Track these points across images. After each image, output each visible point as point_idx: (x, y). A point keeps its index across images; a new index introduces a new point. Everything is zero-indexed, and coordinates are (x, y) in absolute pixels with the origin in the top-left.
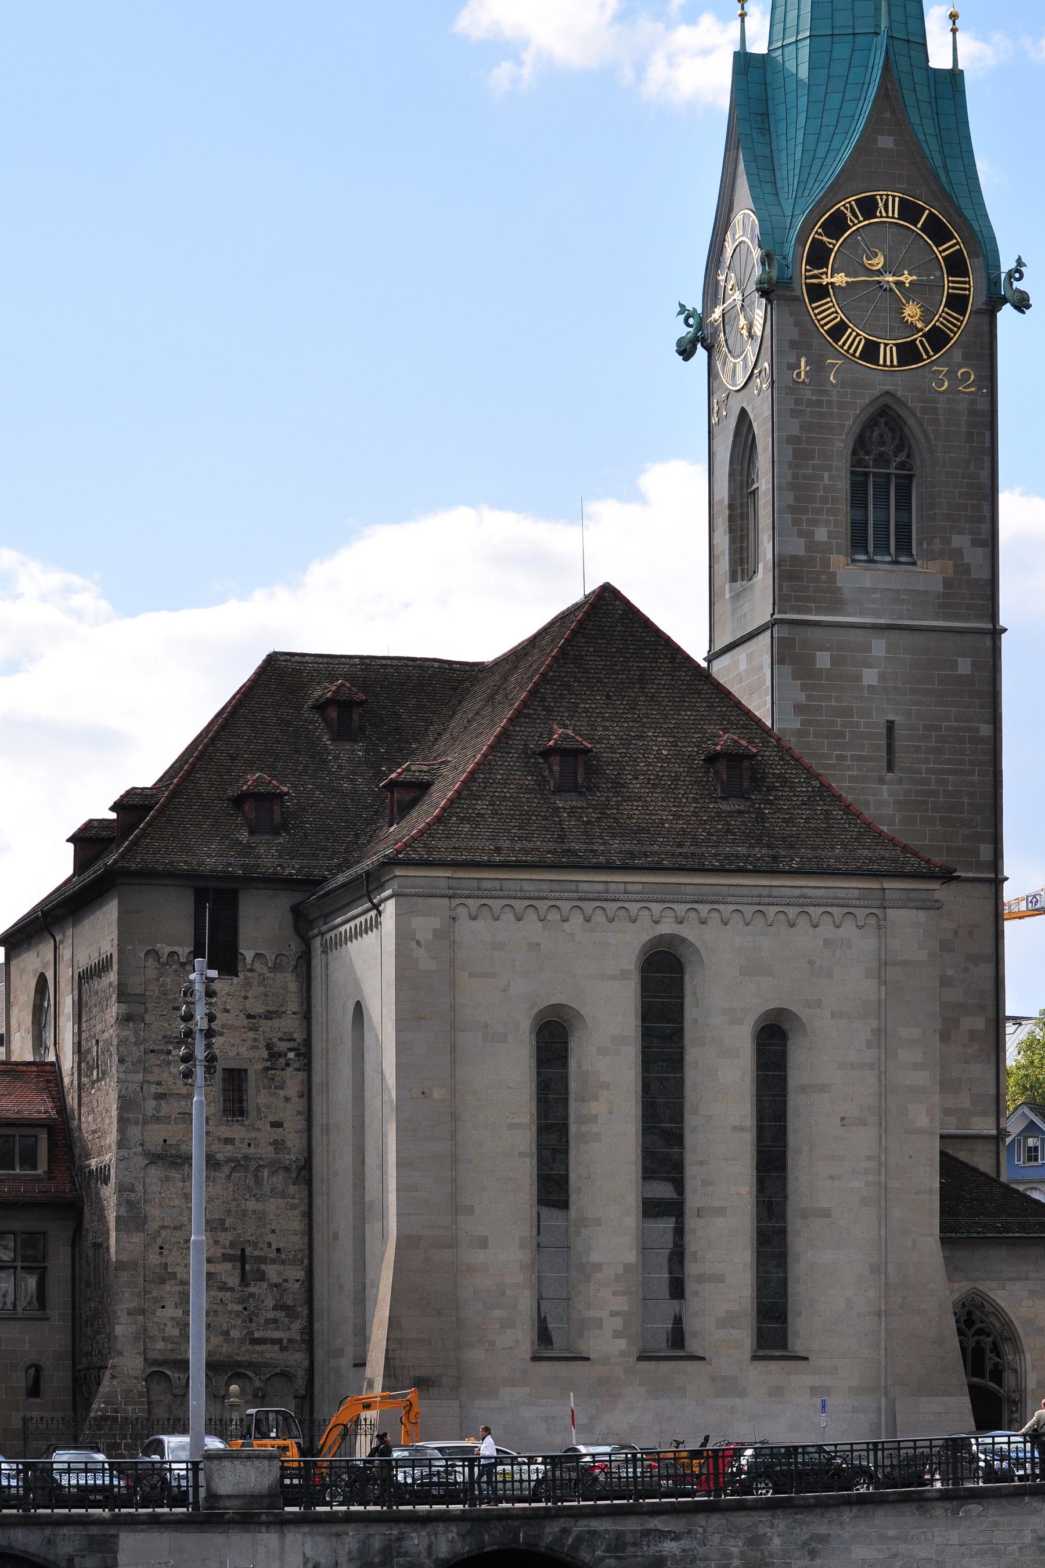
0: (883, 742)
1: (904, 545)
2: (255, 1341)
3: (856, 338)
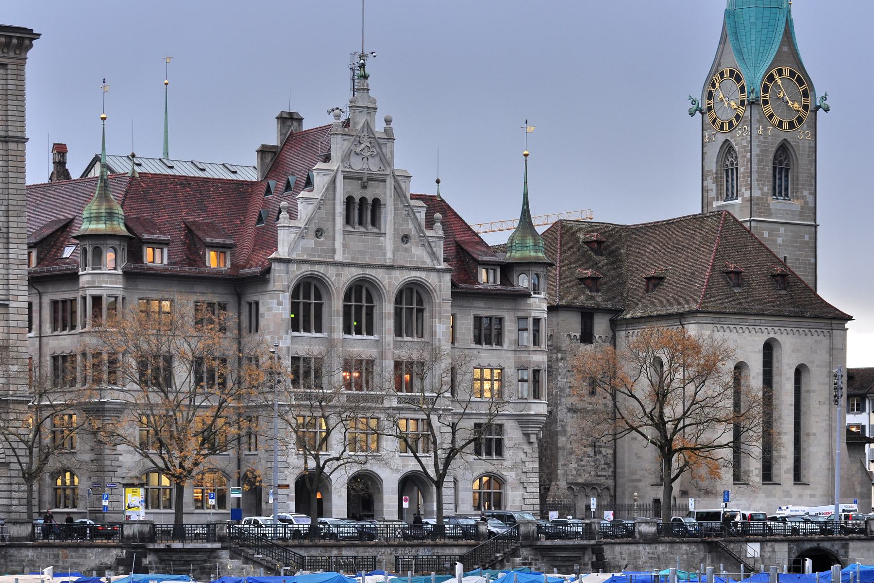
1: (787, 194)
2: (599, 476)
3: (776, 119)
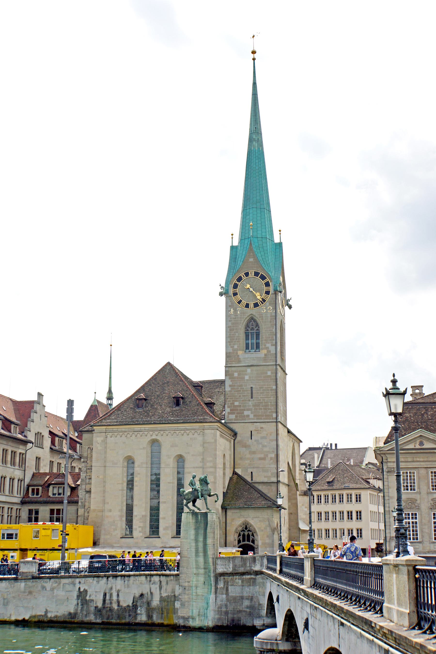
0: (250, 392)
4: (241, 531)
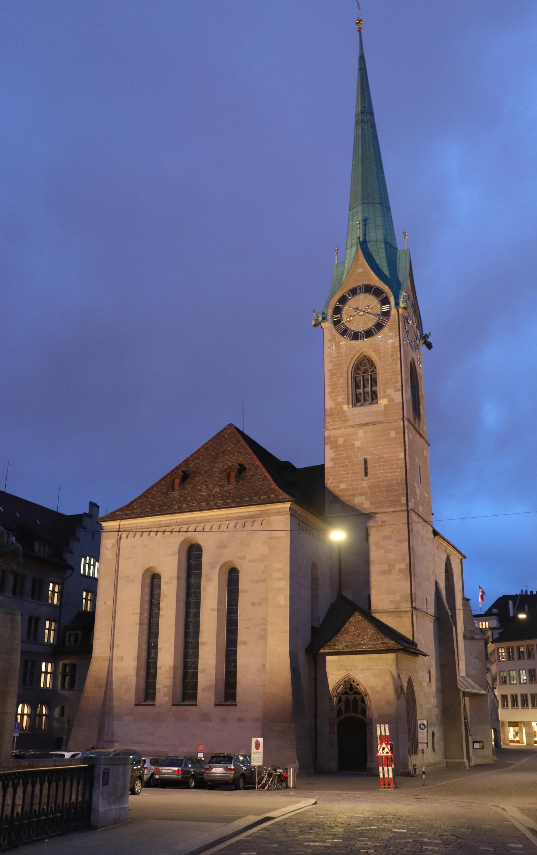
0: (363, 466)
4: (343, 694)
